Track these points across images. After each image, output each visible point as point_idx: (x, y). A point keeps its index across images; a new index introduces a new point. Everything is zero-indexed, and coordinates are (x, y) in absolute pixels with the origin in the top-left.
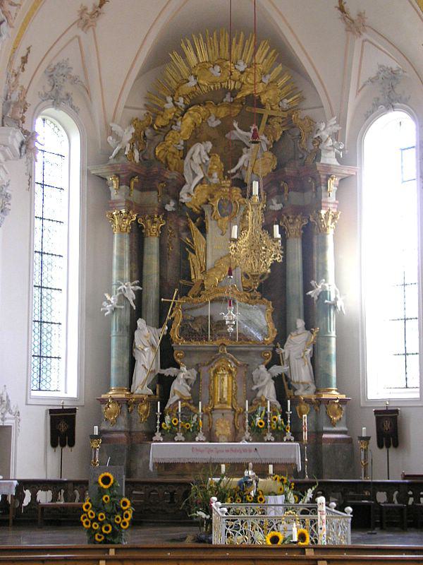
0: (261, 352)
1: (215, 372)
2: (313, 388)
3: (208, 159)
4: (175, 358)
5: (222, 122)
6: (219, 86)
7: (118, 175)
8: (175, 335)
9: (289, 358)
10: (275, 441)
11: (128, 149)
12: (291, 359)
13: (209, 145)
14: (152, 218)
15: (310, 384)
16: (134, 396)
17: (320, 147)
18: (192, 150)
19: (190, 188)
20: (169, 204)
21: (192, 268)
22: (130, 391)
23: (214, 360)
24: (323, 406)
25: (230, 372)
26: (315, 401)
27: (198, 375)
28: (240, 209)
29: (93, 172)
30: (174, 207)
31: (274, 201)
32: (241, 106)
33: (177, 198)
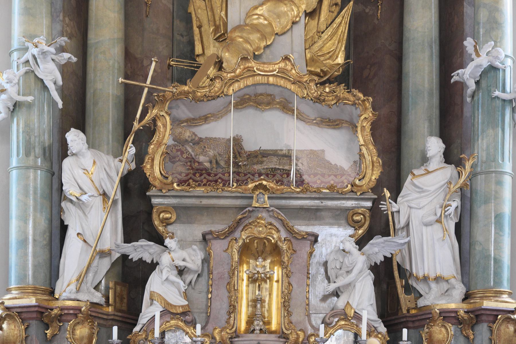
9: (407, 225)
15: (453, 281)
21: (196, 30)
27: (206, 261)
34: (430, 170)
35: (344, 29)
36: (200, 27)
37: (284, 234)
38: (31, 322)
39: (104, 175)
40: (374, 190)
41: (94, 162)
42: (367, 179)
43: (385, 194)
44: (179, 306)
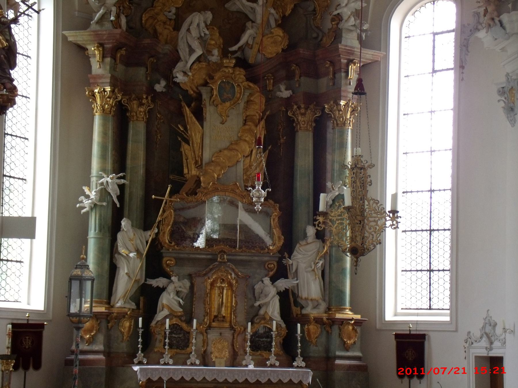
0: (264, 263)
1: (212, 284)
2: (323, 306)
3: (207, 32)
4: (165, 265)
7: (101, 45)
8: (166, 239)
10: (280, 366)
11: (114, 13)
12: (300, 271)
13: (209, 15)
14: (139, 98)
16: (115, 310)
17: (340, 26)
18: (189, 20)
19: (185, 66)
20: (159, 83)
22: (109, 303)
23: (211, 270)
24: (336, 328)
25: (230, 285)
26: (327, 322)
27: (192, 287)
28: (244, 95)
29: (70, 39)
30: (164, 87)
31: (282, 87)
33: (169, 78)
34: (309, 243)
36: (187, 160)
40: (279, 252)
41: (134, 235)
43: (285, 256)
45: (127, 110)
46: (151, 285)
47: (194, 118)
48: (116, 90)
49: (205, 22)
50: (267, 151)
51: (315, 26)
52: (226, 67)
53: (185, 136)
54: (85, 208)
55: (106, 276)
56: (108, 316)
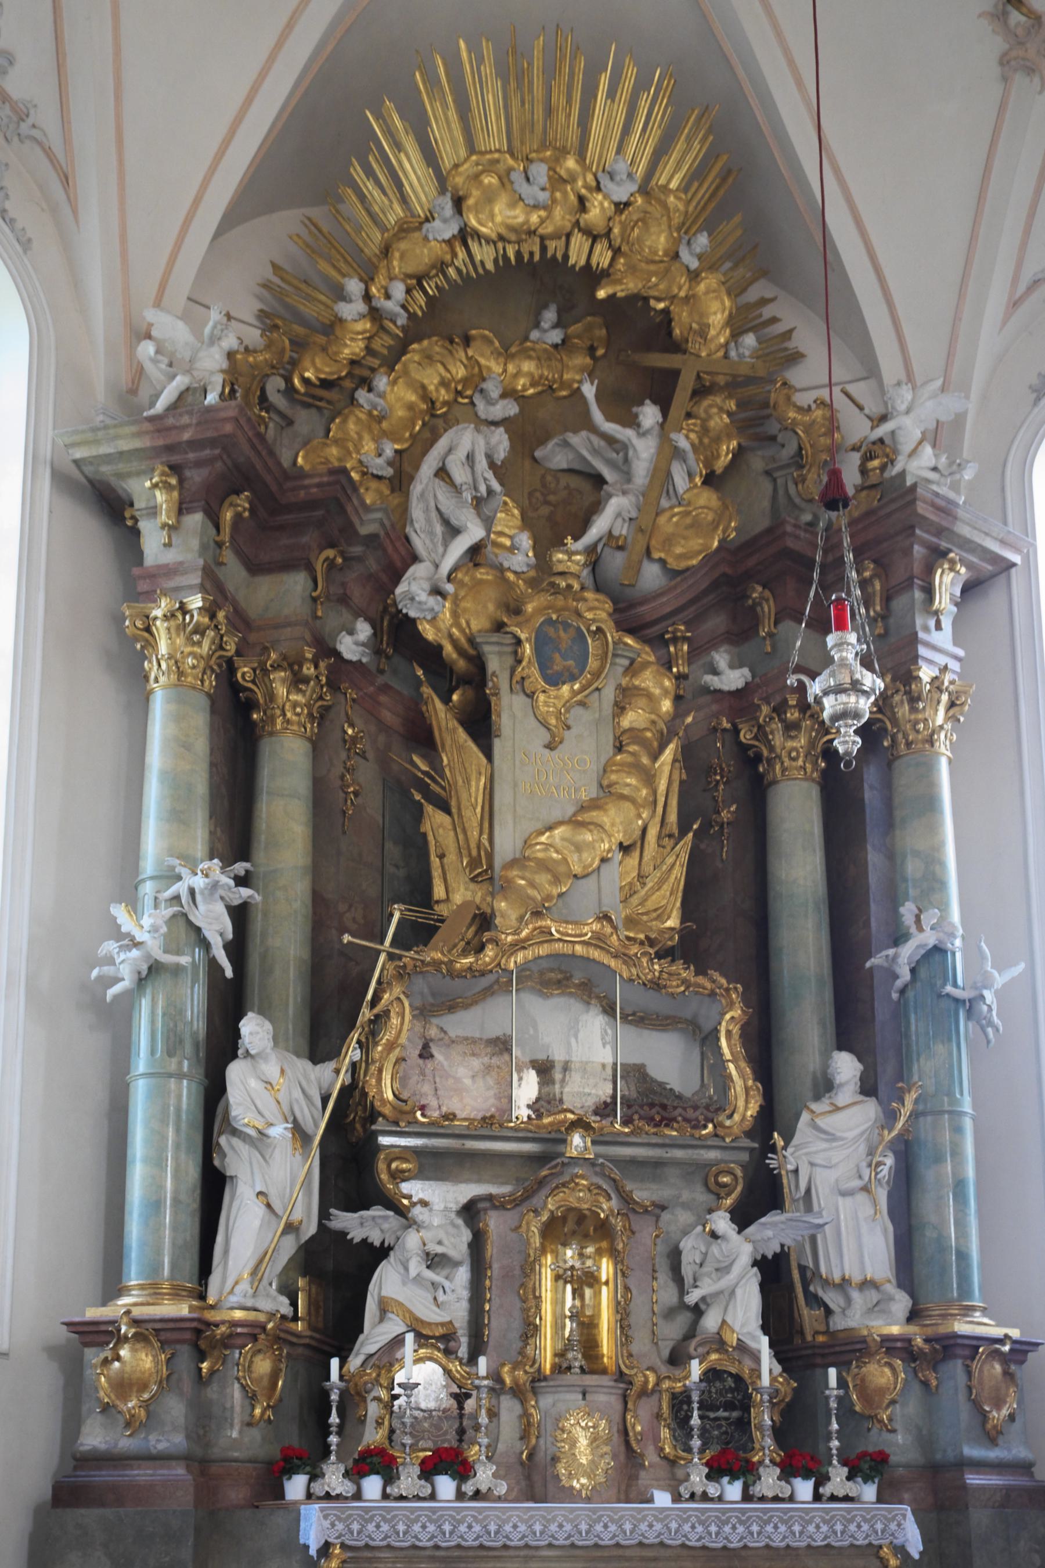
0: (708, 1165)
4: (384, 1177)
5: (522, 410)
6: (536, 249)
18: (442, 444)
21: (435, 861)
22: (202, 1297)
31: (721, 658)
32: (588, 360)
35: (679, 873)
36: (441, 857)
37: (614, 1203)
38: (178, 1347)
39: (297, 1094)
41: (282, 1071)
42: (737, 1117)
43: (775, 1143)
44: (437, 1324)
45: (251, 705)
46: (343, 1234)
47: (461, 730)
48: (221, 615)
49: (489, 457)
50: (691, 835)
51: (803, 499)
52: (562, 574)
53: (433, 786)
54: (118, 980)
55: (192, 1202)
56: (198, 1332)
